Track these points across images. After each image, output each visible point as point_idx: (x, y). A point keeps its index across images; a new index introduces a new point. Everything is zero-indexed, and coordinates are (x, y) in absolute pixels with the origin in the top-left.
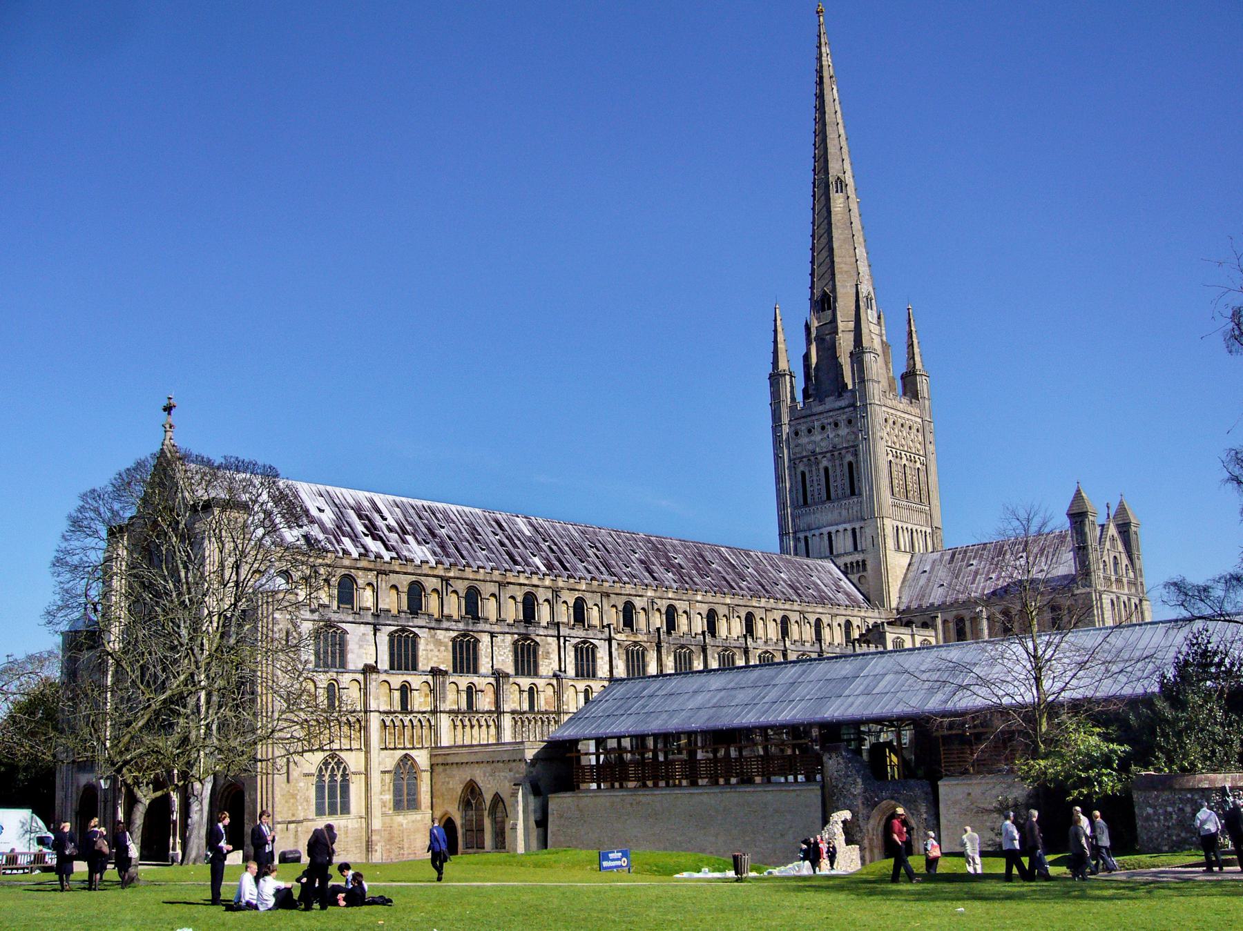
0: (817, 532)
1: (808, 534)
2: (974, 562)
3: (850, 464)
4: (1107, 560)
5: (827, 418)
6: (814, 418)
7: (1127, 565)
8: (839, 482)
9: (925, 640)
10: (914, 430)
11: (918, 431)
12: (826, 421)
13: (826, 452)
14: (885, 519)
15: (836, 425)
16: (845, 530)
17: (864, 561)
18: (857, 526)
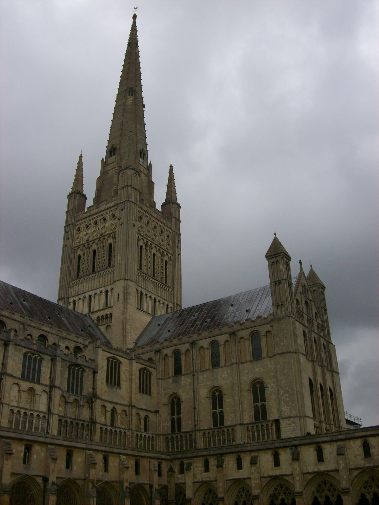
0: (82, 297)
1: (76, 299)
2: (196, 315)
3: (110, 245)
4: (300, 300)
5: (98, 217)
6: (91, 218)
7: (316, 313)
8: (101, 260)
9: (145, 369)
10: (165, 234)
11: (168, 236)
12: (98, 219)
13: (95, 239)
14: (129, 281)
15: (104, 219)
16: (101, 292)
17: (111, 314)
18: (109, 288)
